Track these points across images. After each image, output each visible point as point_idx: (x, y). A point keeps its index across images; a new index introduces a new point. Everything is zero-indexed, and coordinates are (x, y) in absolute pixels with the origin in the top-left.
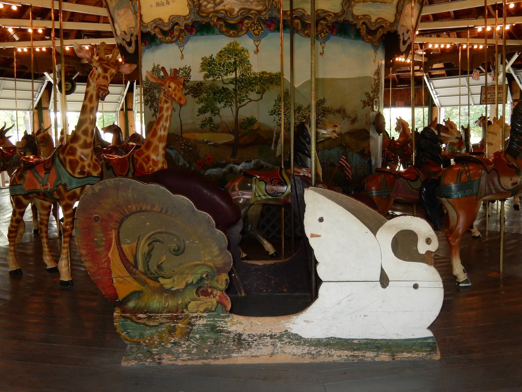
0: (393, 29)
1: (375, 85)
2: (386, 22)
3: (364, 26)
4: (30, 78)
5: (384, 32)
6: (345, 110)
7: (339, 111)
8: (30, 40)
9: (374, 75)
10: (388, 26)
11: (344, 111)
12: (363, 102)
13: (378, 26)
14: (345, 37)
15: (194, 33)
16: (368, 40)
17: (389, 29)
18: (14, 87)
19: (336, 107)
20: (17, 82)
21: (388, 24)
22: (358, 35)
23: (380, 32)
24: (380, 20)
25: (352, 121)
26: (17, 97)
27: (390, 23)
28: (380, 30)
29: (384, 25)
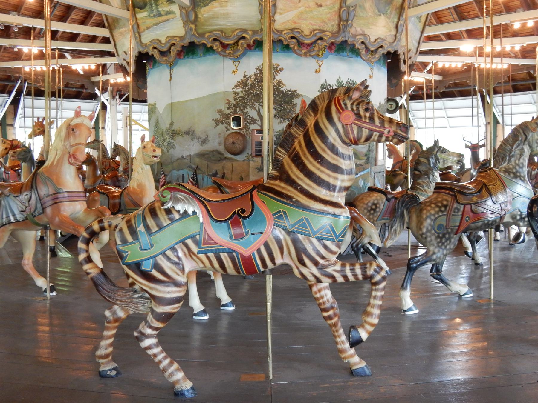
0: (185, 42)
1: (235, 99)
2: (175, 38)
3: (155, 50)
4: (470, 96)
5: (178, 49)
6: (194, 131)
7: (187, 133)
8: (483, 57)
9: (234, 88)
10: (178, 41)
11: (193, 132)
12: (215, 121)
13: (169, 45)
14: (193, 58)
15: (333, 51)
16: (165, 61)
17: (182, 44)
18: (432, 107)
19: (184, 129)
20: (435, 102)
21: (178, 39)
22: (209, 50)
23: (172, 50)
24: (168, 39)
25: (202, 141)
26: (436, 115)
27: (179, 37)
28: (172, 48)
29: (174, 42)
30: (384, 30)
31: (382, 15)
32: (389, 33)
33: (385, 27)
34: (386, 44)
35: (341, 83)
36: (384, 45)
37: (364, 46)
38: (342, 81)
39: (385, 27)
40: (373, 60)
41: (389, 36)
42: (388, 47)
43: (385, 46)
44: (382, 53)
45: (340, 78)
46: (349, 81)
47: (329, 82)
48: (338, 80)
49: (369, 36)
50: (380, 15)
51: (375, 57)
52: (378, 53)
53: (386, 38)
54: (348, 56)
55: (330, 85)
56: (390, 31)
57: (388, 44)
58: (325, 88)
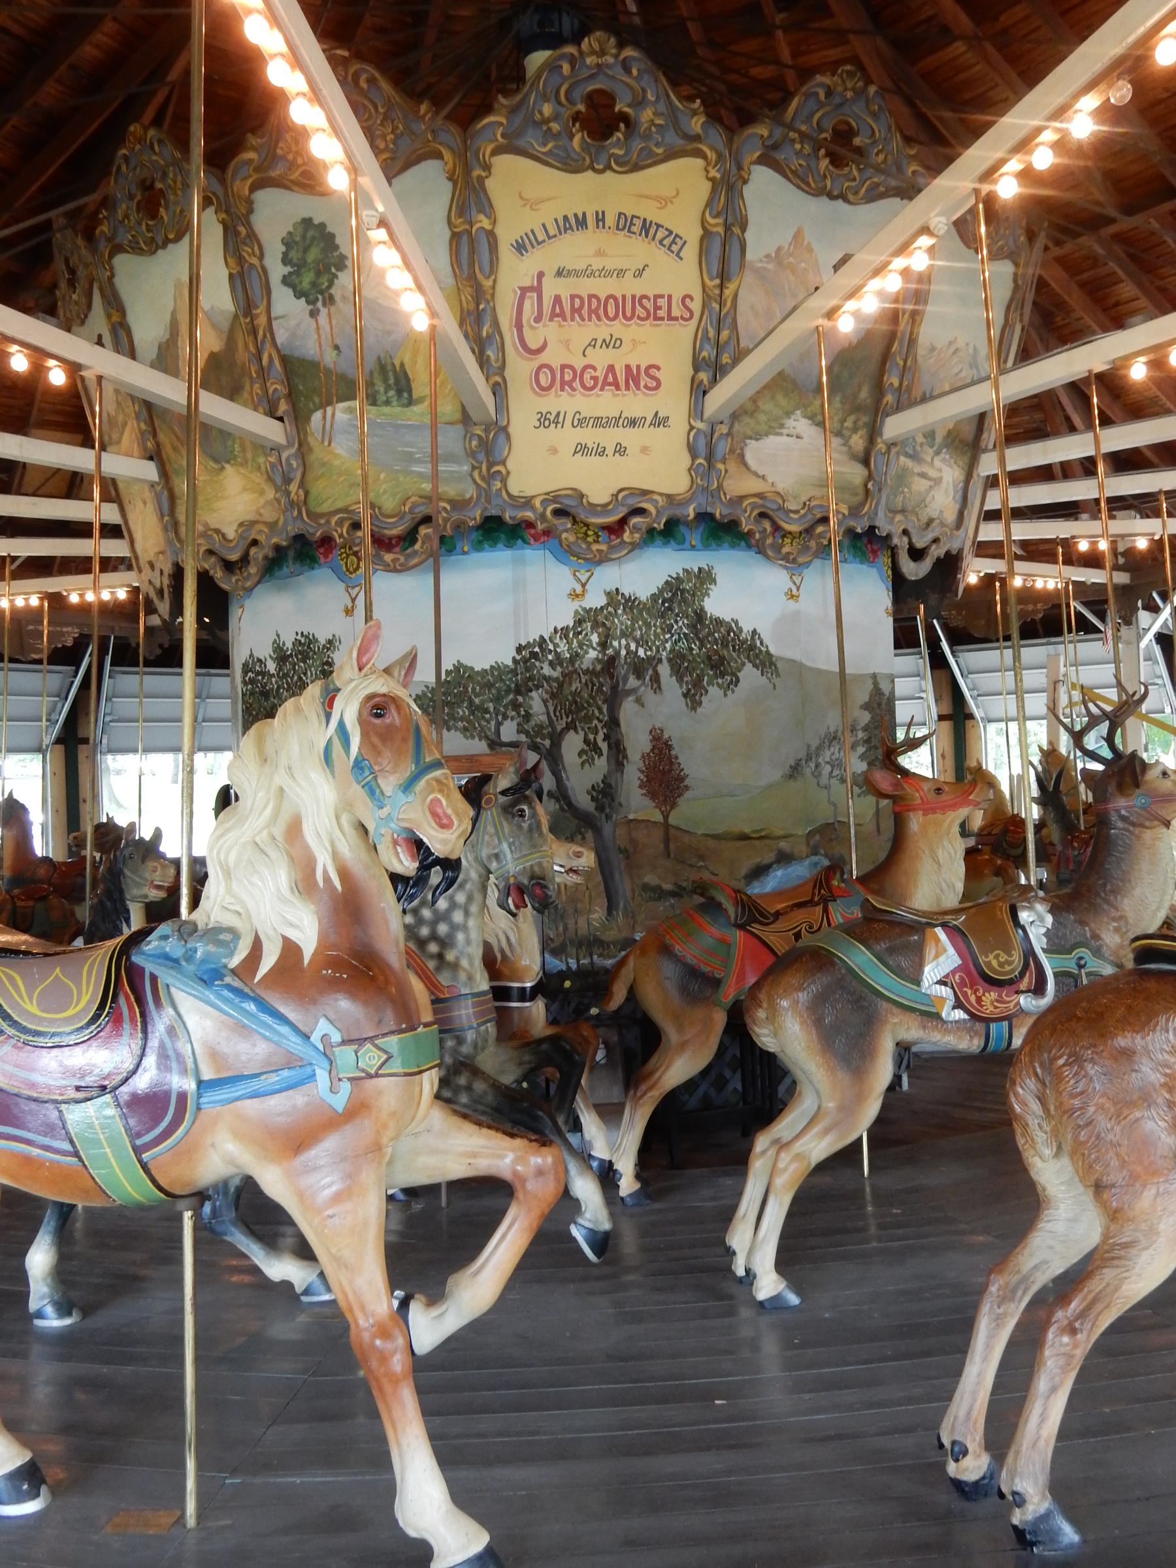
30: (248, 497)
31: (227, 466)
32: (262, 501)
33: (244, 490)
34: (260, 532)
35: (281, 649)
36: (258, 538)
37: (213, 559)
38: (284, 644)
39: (244, 490)
40: (248, 584)
41: (263, 507)
42: (268, 537)
43: (262, 538)
44: (260, 556)
45: (278, 635)
46: (299, 637)
47: (256, 654)
48: (275, 642)
49: (217, 531)
50: (223, 468)
51: (249, 574)
52: (252, 562)
53: (261, 515)
54: (293, 574)
55: (259, 660)
56: (262, 493)
57: (266, 530)
58: (251, 671)
